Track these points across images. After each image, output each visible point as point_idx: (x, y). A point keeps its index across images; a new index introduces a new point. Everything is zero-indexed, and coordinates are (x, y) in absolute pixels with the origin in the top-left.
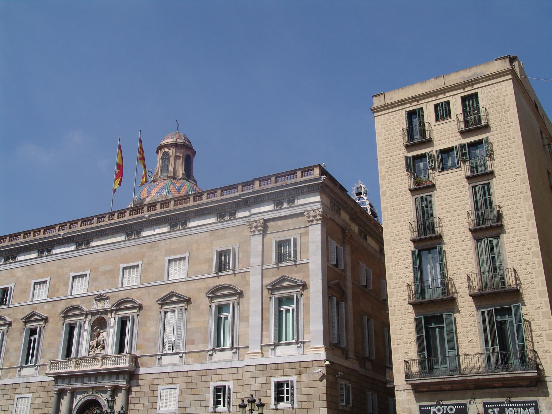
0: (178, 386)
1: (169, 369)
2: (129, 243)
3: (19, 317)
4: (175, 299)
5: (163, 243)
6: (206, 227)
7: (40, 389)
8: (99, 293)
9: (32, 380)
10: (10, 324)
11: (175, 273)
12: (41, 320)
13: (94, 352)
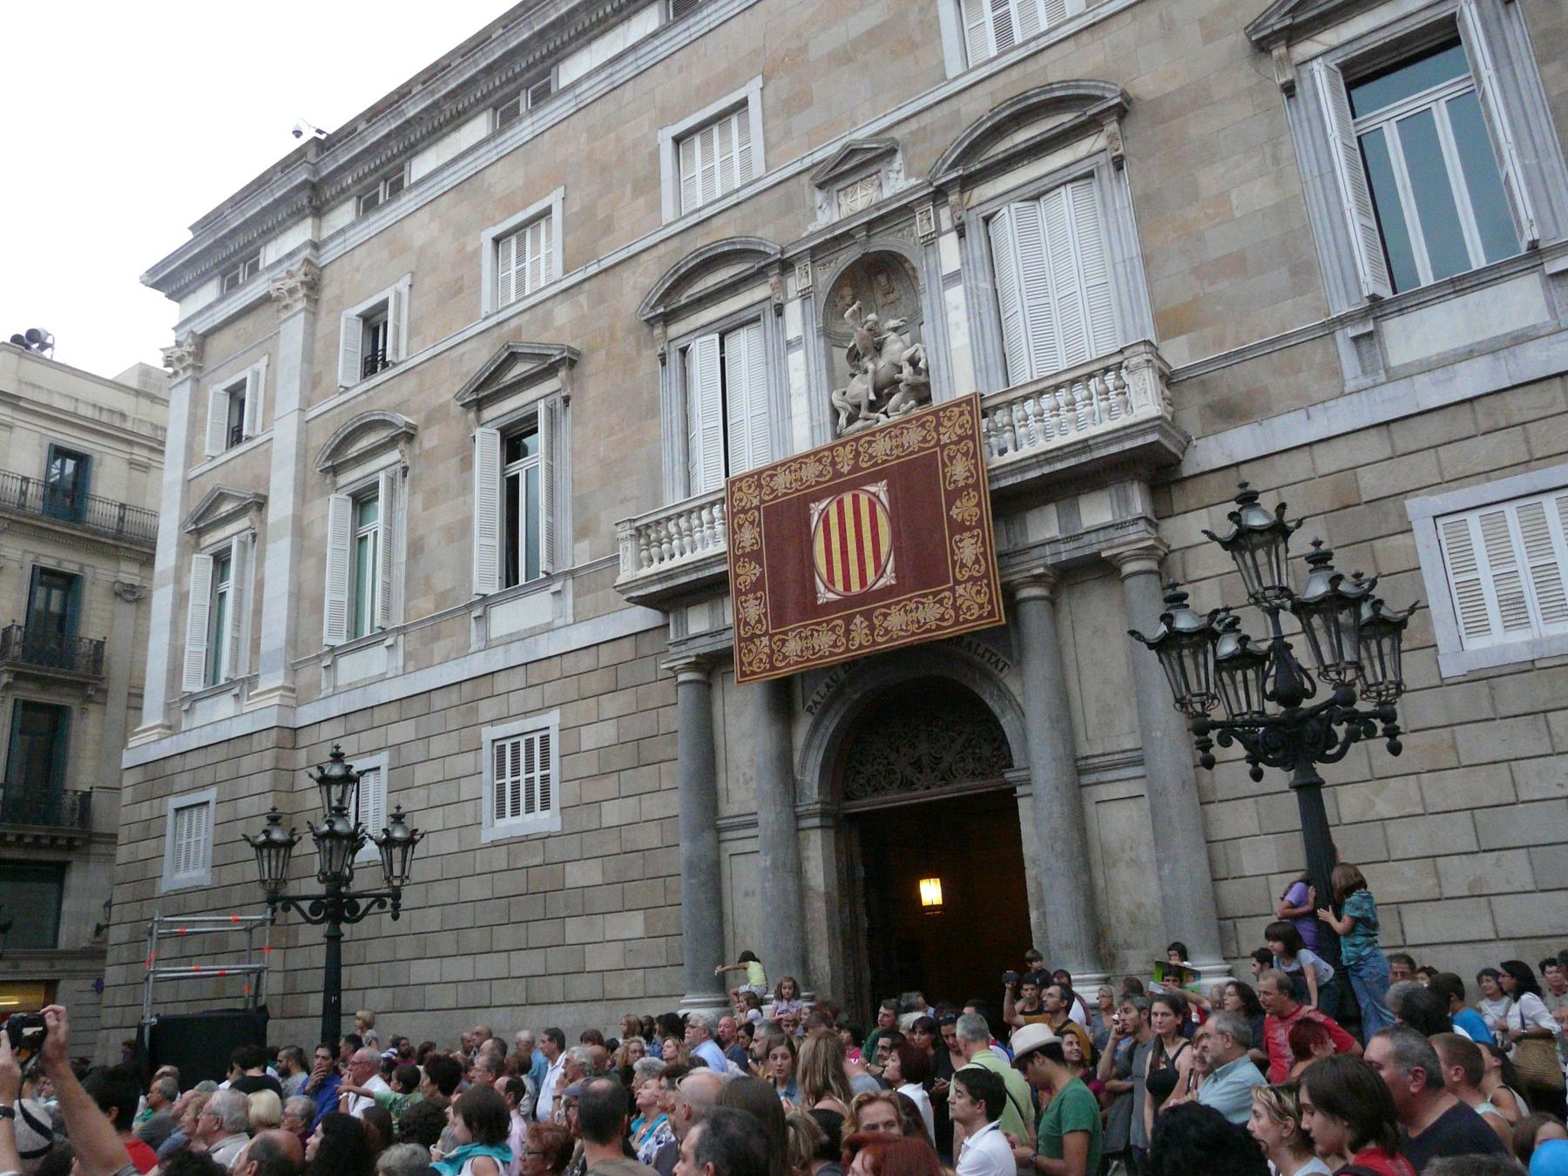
1: (1472, 380)
7: (593, 683)
8: (833, 149)
9: (548, 646)
10: (409, 436)
12: (550, 371)
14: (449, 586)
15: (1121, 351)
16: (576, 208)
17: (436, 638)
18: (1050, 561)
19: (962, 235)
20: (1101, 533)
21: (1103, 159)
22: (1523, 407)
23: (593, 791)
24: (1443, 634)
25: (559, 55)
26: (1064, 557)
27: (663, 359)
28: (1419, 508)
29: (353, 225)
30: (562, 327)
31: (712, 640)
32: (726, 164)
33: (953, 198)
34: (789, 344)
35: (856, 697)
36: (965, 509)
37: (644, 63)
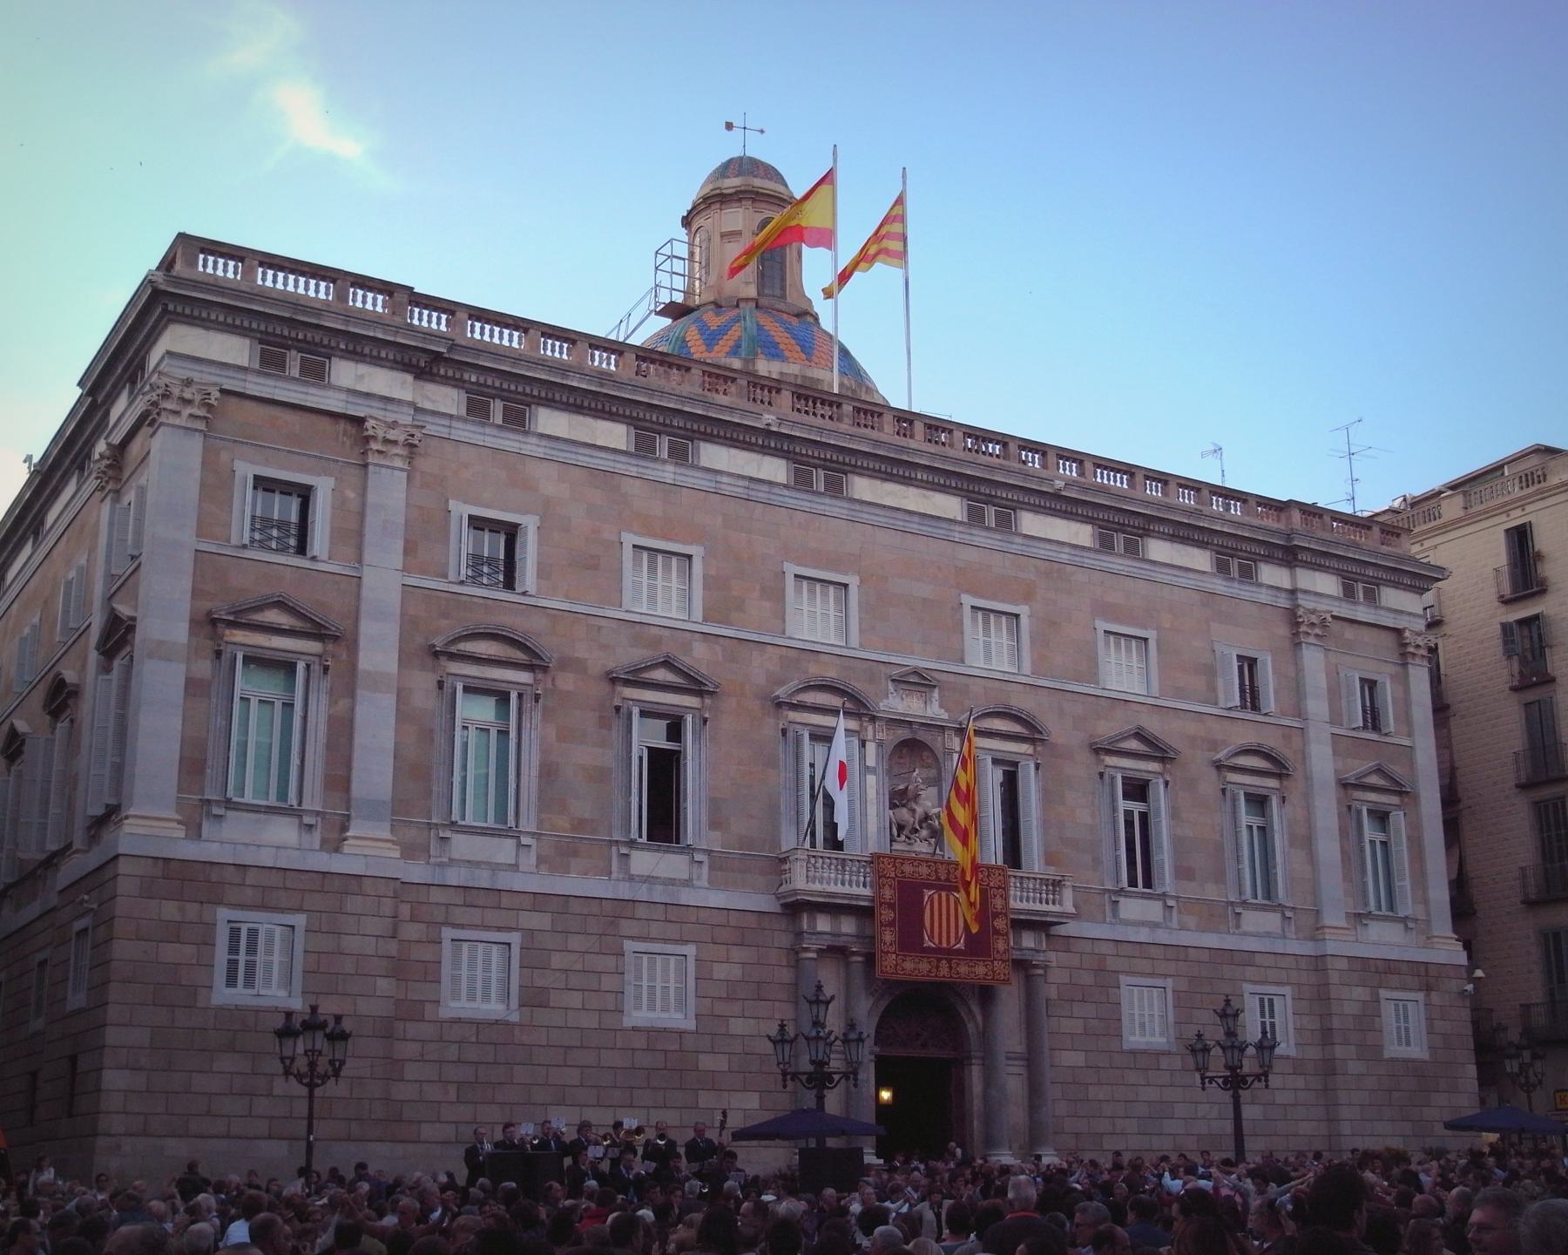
0: (1169, 983)
1: (1143, 935)
2: (979, 537)
3: (581, 651)
4: (1133, 745)
5: (1081, 576)
6: (1191, 575)
9: (687, 897)
11: (1120, 674)
14: (587, 816)
16: (713, 573)
17: (575, 854)
22: (1154, 951)
23: (720, 1008)
24: (1125, 1032)
25: (710, 438)
28: (1123, 979)
29: (459, 418)
30: (699, 657)
32: (826, 616)
36: (1000, 924)
37: (776, 499)
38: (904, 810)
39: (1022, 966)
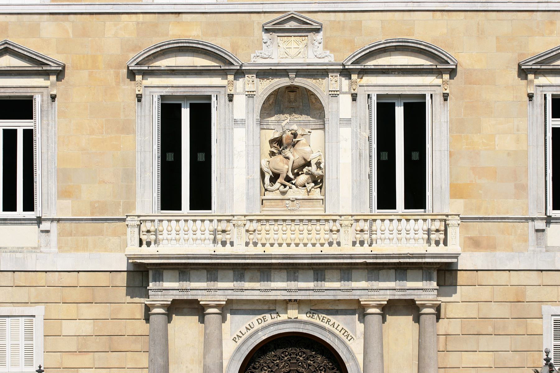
7: (75, 294)
12: (46, 74)
13: (283, 193)
15: (447, 216)
18: (388, 298)
19: (354, 97)
20: (416, 291)
21: (439, 91)
26: (397, 297)
27: (139, 98)
31: (181, 293)
33: (354, 77)
34: (235, 121)
35: (264, 338)
38: (279, 158)
39: (410, 307)
